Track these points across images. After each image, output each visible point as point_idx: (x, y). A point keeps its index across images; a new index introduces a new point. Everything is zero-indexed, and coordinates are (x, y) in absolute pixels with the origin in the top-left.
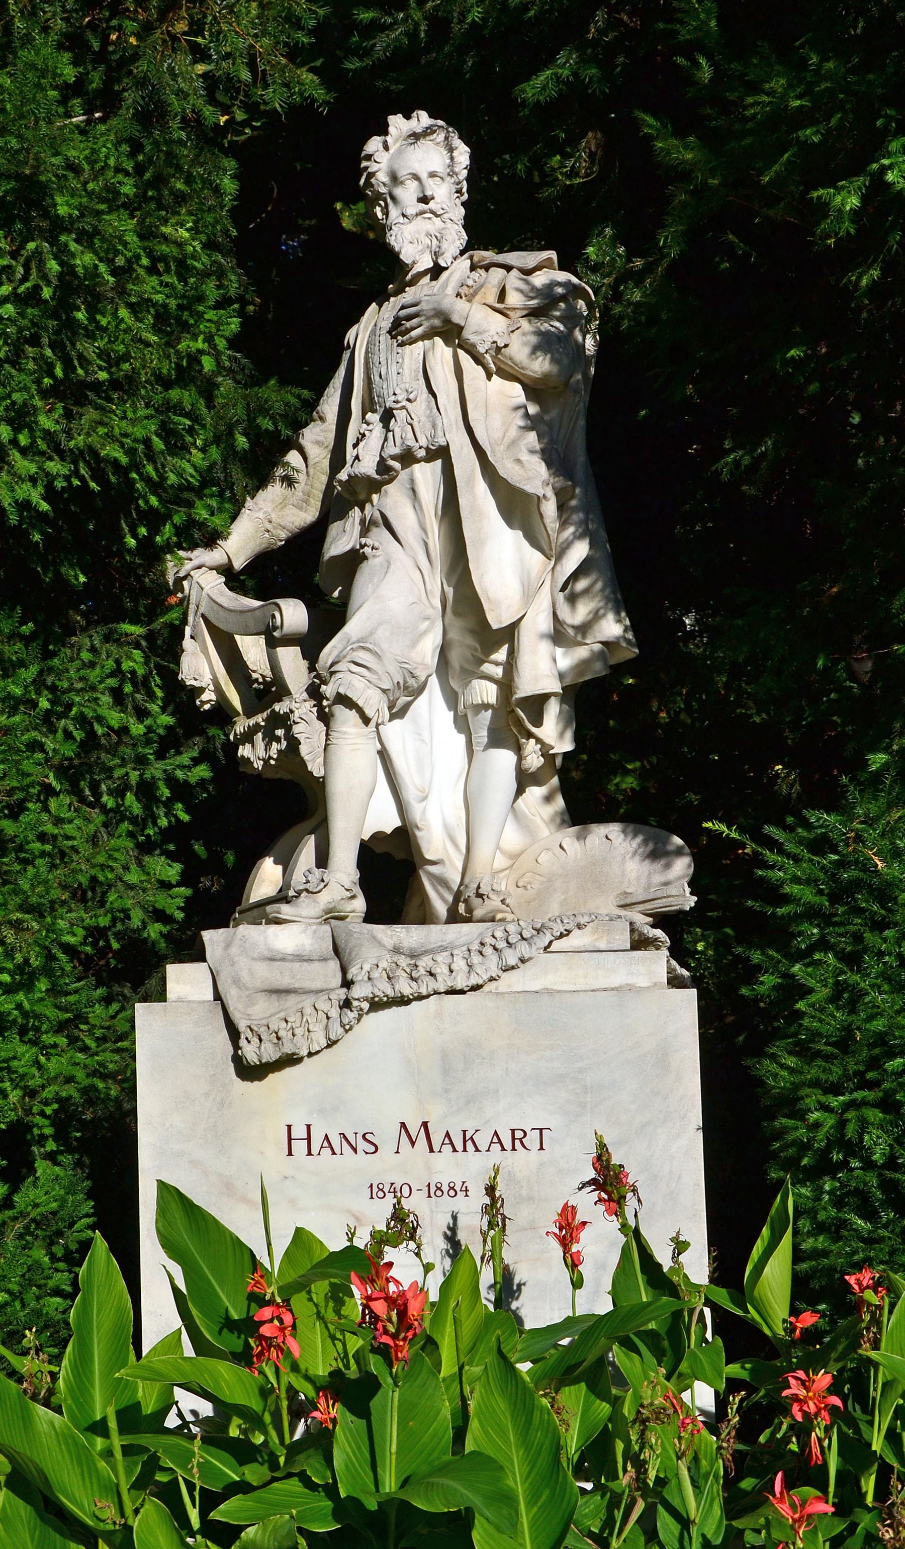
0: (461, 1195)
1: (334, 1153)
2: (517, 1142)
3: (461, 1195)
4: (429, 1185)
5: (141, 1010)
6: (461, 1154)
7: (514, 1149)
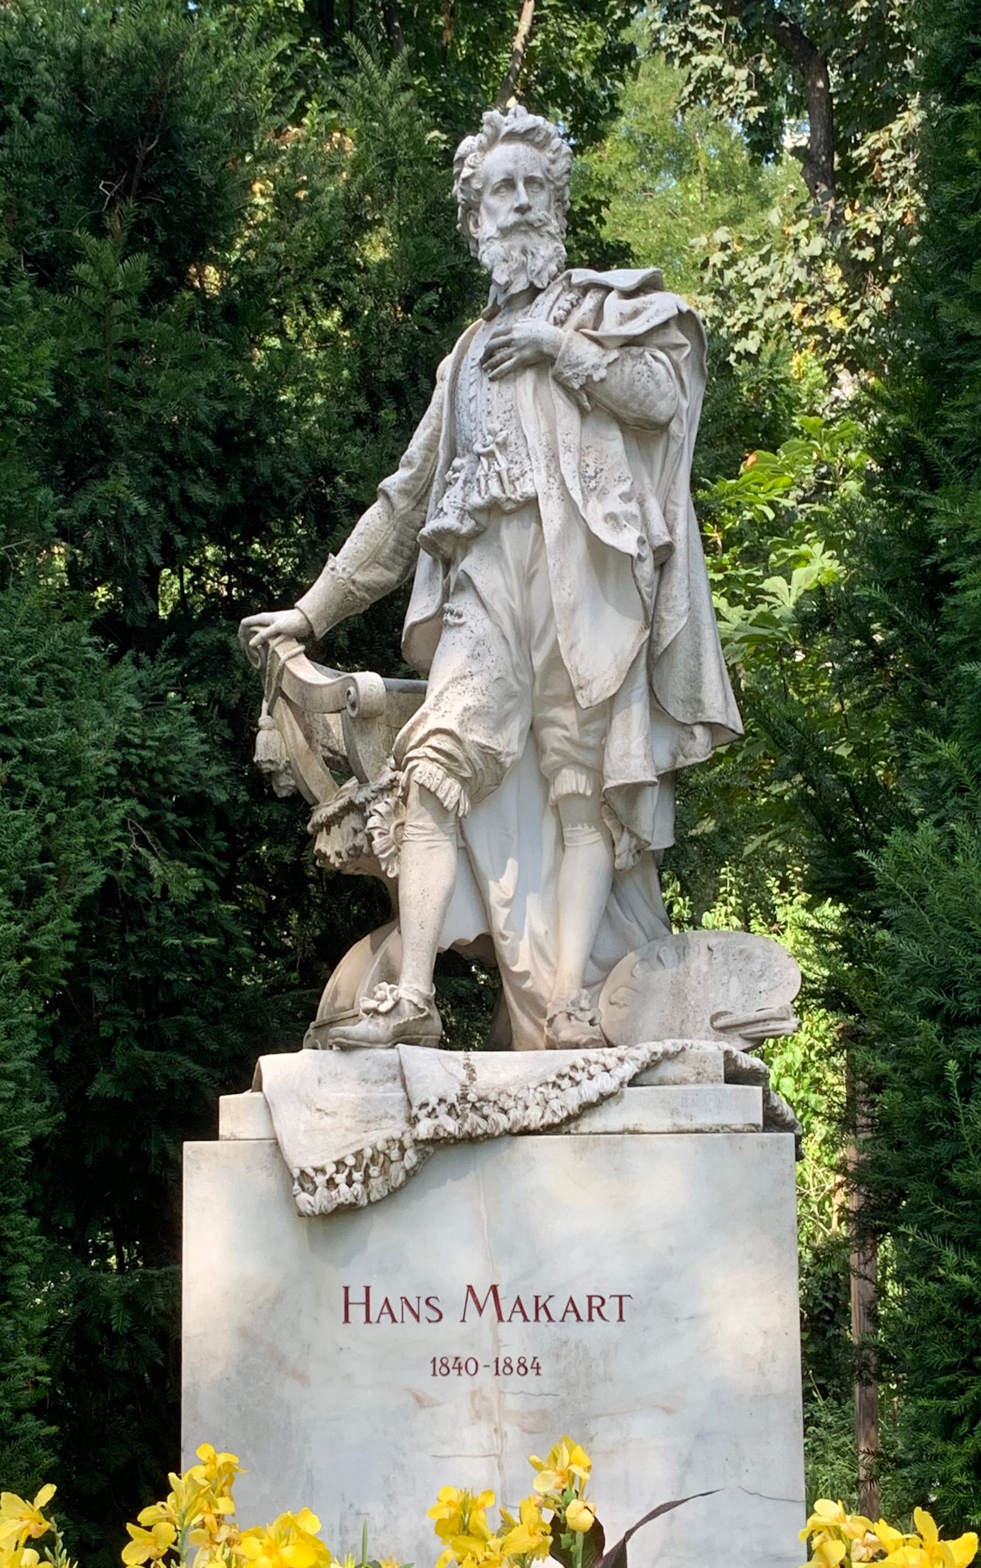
1: (394, 1320)
2: (595, 1312)
3: (532, 1372)
4: (497, 1361)
5: (190, 1148)
6: (531, 1325)
7: (590, 1319)
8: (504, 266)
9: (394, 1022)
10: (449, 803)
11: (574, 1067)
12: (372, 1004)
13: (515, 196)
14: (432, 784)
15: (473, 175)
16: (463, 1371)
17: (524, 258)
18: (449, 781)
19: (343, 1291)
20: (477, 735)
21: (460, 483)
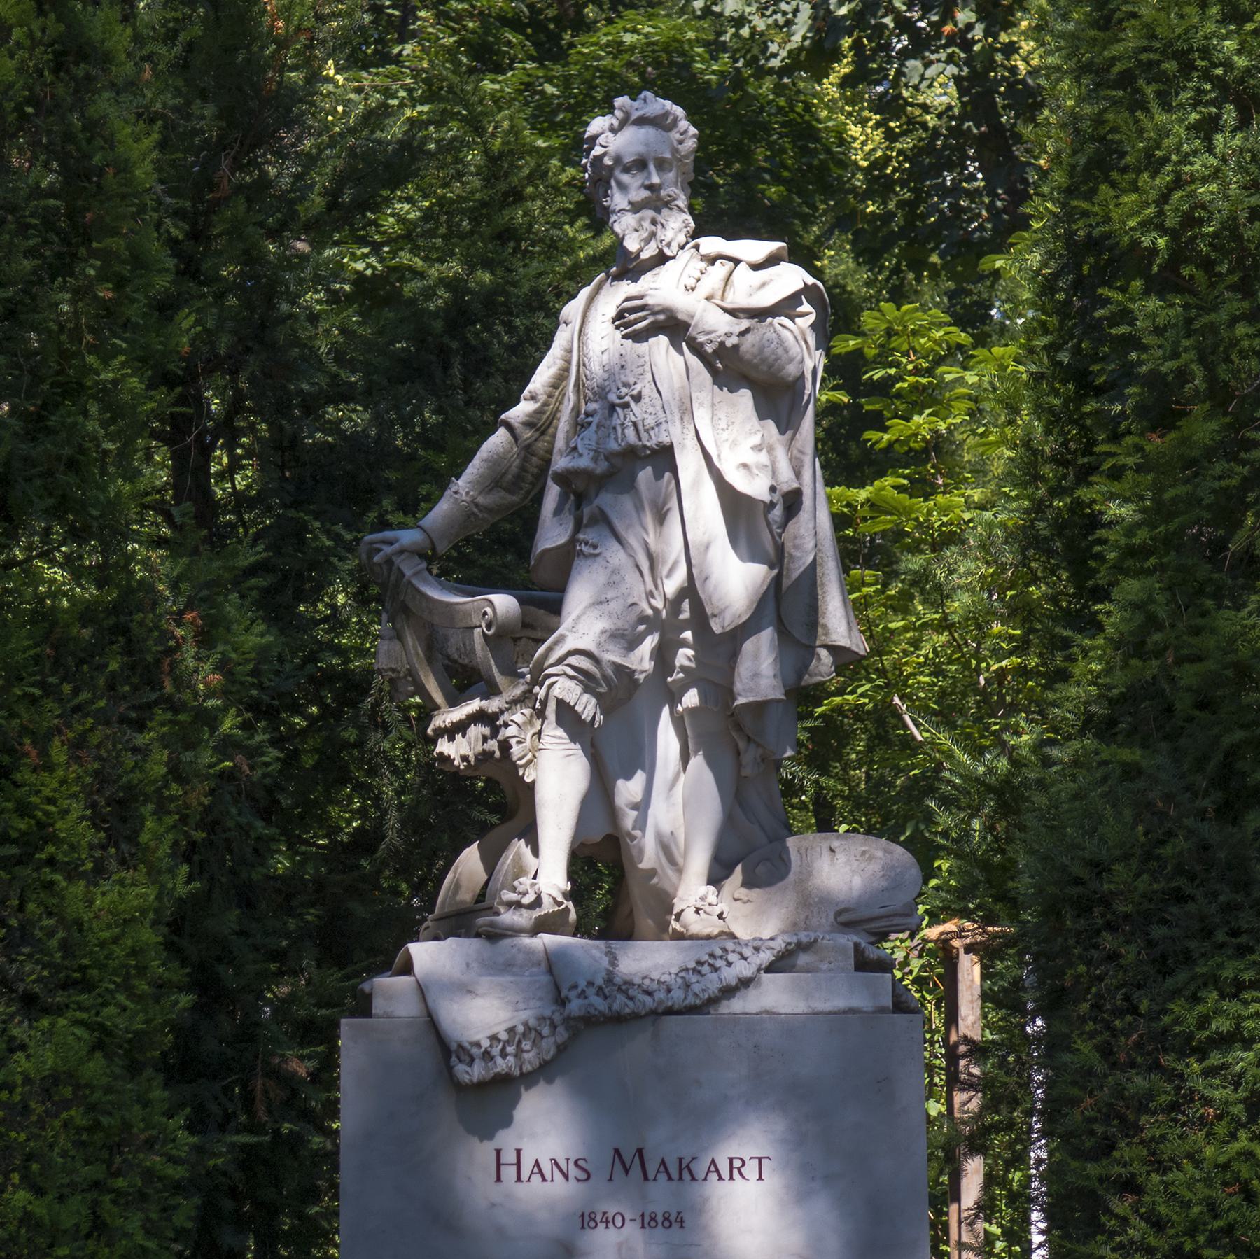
0: (676, 1226)
1: (544, 1179)
2: (735, 1172)
3: (676, 1226)
4: (643, 1215)
6: (674, 1184)
8: (636, 234)
9: (537, 913)
10: (587, 715)
11: (712, 955)
12: (513, 896)
13: (645, 174)
14: (571, 699)
15: (605, 154)
16: (611, 1225)
17: (653, 228)
18: (586, 697)
19: (495, 1153)
20: (612, 655)
21: (593, 427)
